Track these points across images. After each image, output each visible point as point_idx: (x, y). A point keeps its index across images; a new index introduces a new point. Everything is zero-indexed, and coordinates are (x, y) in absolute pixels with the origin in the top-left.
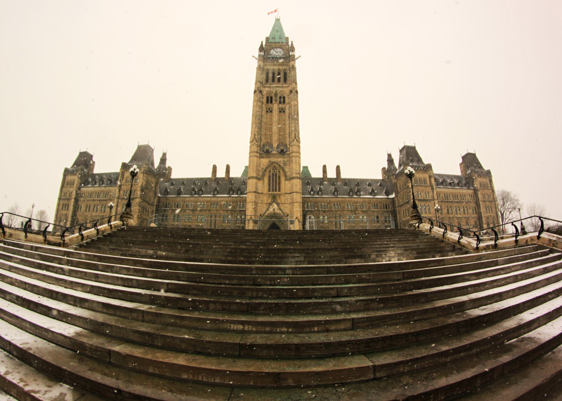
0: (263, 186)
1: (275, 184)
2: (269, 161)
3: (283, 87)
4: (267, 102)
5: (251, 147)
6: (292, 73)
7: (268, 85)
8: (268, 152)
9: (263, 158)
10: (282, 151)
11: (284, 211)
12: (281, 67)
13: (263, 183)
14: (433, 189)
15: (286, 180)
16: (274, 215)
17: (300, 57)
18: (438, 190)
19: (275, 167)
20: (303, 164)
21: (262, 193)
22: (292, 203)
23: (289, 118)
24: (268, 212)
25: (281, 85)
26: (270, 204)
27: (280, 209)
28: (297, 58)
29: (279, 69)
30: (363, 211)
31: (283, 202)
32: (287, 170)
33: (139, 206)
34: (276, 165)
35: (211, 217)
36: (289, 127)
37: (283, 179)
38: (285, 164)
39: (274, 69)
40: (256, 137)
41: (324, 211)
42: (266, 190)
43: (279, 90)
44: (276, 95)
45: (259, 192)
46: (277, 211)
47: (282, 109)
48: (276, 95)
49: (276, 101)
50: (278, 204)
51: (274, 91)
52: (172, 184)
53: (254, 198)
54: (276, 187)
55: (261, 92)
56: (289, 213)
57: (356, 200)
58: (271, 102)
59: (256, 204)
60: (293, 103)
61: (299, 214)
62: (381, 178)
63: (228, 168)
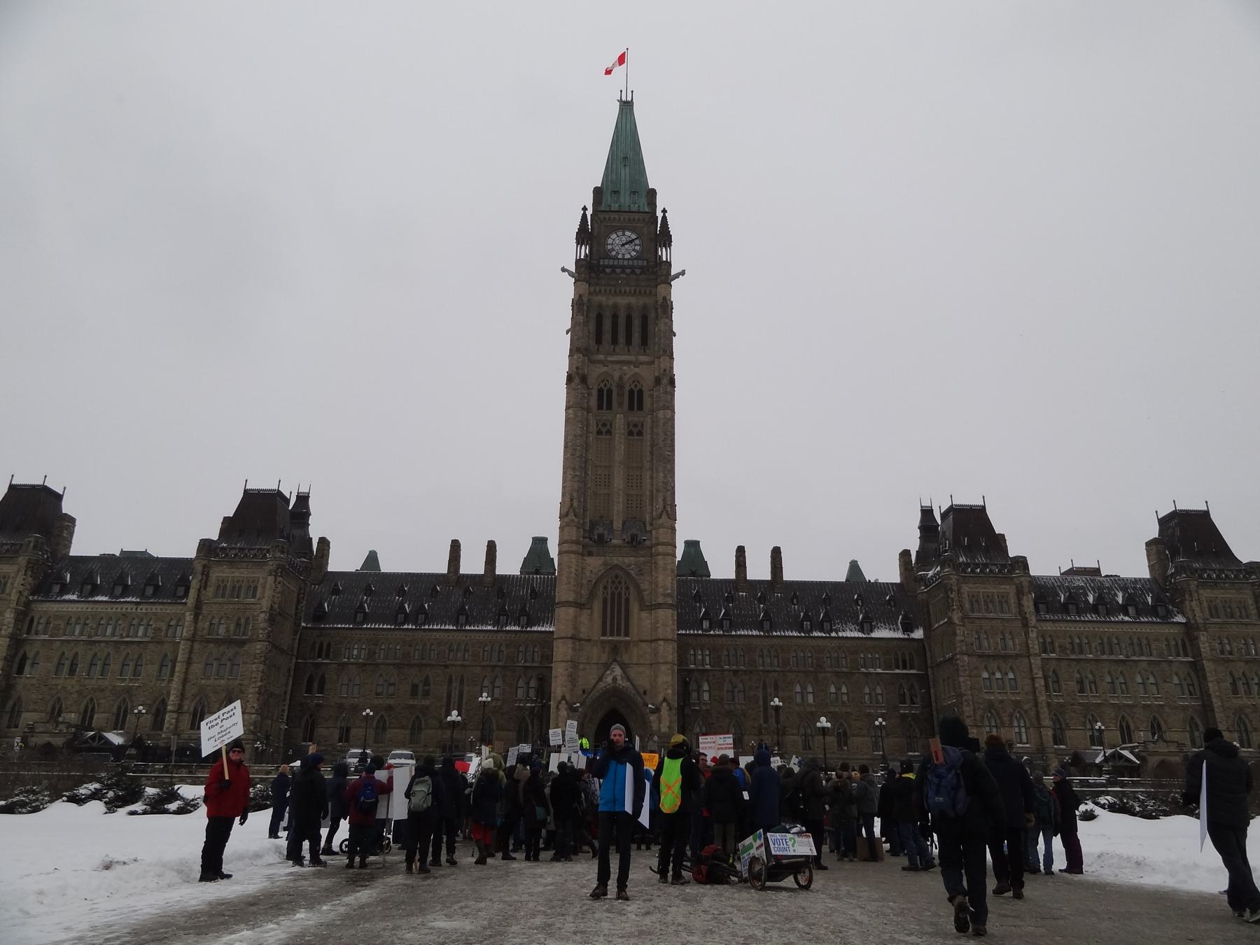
0: (590, 623)
1: (616, 619)
2: (605, 564)
3: (637, 364)
4: (600, 407)
5: (561, 528)
7: (601, 357)
8: (601, 540)
9: (590, 554)
10: (634, 537)
12: (633, 300)
13: (591, 615)
14: (1025, 625)
17: (683, 273)
18: (1048, 627)
19: (617, 577)
20: (684, 532)
22: (654, 665)
23: (652, 453)
24: (602, 685)
25: (632, 358)
26: (607, 666)
27: (629, 679)
28: (677, 276)
29: (629, 306)
30: (837, 674)
31: (635, 661)
32: (645, 586)
35: (450, 681)
36: (652, 478)
37: (635, 606)
38: (641, 573)
39: (615, 306)
40: (575, 504)
41: (736, 672)
43: (630, 371)
45: (582, 636)
47: (636, 426)
48: (621, 386)
49: (621, 404)
50: (624, 667)
51: (616, 375)
52: (336, 591)
53: (570, 651)
54: (619, 624)
55: (584, 379)
57: (820, 643)
58: (609, 407)
59: (574, 663)
60: (661, 414)
61: (670, 691)
62: (898, 580)
63: (491, 547)
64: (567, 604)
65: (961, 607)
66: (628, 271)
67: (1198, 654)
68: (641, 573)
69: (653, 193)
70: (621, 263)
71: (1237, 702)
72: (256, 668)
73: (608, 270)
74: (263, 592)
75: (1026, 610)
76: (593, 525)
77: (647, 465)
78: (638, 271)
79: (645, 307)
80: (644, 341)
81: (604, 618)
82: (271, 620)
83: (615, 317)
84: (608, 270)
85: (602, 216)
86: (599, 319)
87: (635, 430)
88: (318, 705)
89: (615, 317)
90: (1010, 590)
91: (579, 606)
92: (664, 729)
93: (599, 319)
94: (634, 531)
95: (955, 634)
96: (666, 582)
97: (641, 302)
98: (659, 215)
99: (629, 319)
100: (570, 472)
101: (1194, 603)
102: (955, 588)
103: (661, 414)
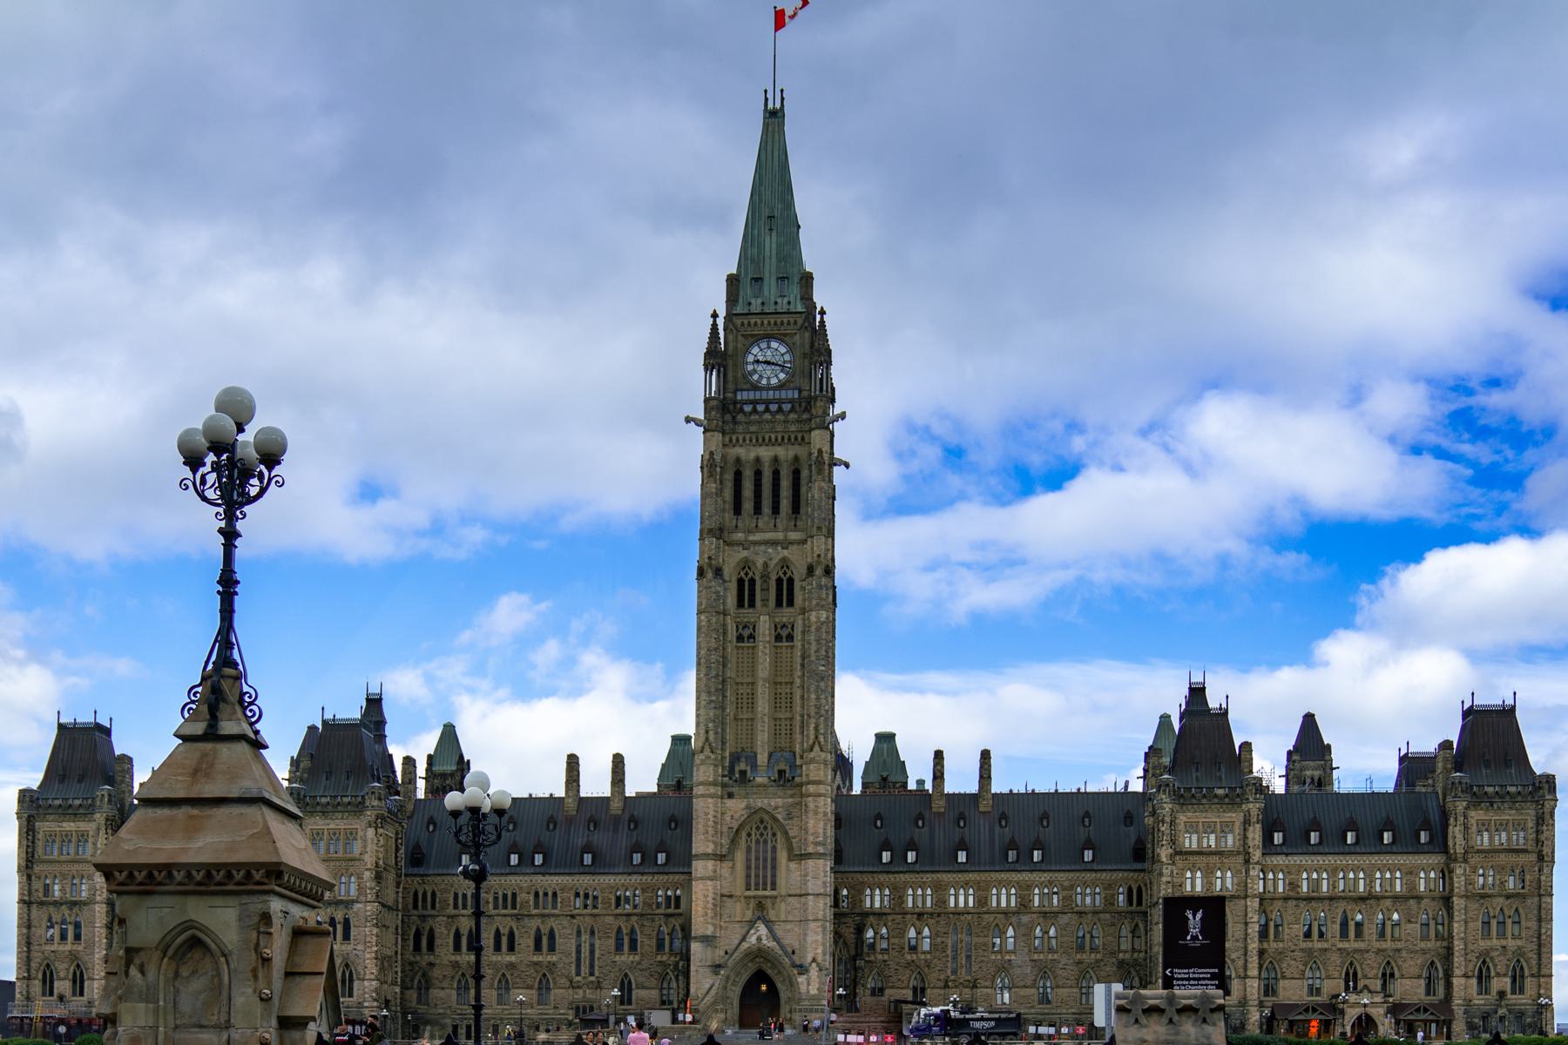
0: (733, 876)
2: (748, 807)
3: (786, 544)
4: (740, 604)
6: (816, 493)
7: (740, 536)
8: (744, 778)
9: (730, 796)
10: (781, 772)
11: (785, 942)
12: (780, 451)
13: (733, 867)
14: (1247, 862)
15: (790, 860)
16: (759, 953)
21: (731, 896)
22: (803, 921)
23: (803, 665)
24: (745, 945)
25: (780, 536)
26: (752, 924)
29: (776, 459)
31: (783, 917)
32: (791, 834)
33: (376, 926)
34: (766, 818)
36: (802, 697)
37: (782, 856)
39: (758, 460)
40: (711, 737)
42: (739, 890)
43: (778, 554)
44: (765, 577)
46: (768, 943)
47: (784, 626)
48: (765, 577)
50: (768, 924)
51: (760, 563)
55: (718, 572)
56: (796, 945)
58: (752, 605)
61: (820, 951)
64: (706, 856)
65: (1173, 842)
66: (774, 407)
67: (1452, 890)
68: (789, 816)
69: (807, 279)
70: (764, 395)
71: (1484, 944)
72: (370, 931)
73: (748, 408)
74: (365, 847)
75: (1251, 843)
76: (735, 758)
77: (798, 681)
78: (787, 407)
79: (796, 458)
80: (796, 508)
81: (748, 868)
82: (378, 877)
83: (758, 474)
84: (748, 408)
85: (738, 322)
86: (738, 476)
87: (784, 633)
88: (431, 965)
89: (758, 474)
90: (1236, 817)
91: (721, 858)
92: (813, 991)
93: (738, 476)
94: (782, 766)
95: (1161, 874)
96: (818, 826)
97: (791, 454)
98: (818, 318)
99: (776, 474)
100: (704, 696)
101: (1457, 829)
102: (1168, 819)
103: (813, 619)
